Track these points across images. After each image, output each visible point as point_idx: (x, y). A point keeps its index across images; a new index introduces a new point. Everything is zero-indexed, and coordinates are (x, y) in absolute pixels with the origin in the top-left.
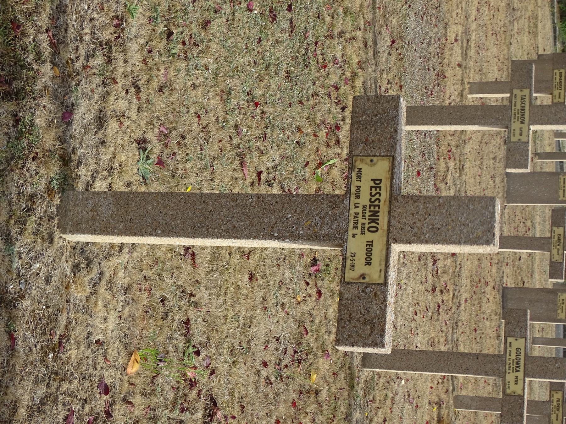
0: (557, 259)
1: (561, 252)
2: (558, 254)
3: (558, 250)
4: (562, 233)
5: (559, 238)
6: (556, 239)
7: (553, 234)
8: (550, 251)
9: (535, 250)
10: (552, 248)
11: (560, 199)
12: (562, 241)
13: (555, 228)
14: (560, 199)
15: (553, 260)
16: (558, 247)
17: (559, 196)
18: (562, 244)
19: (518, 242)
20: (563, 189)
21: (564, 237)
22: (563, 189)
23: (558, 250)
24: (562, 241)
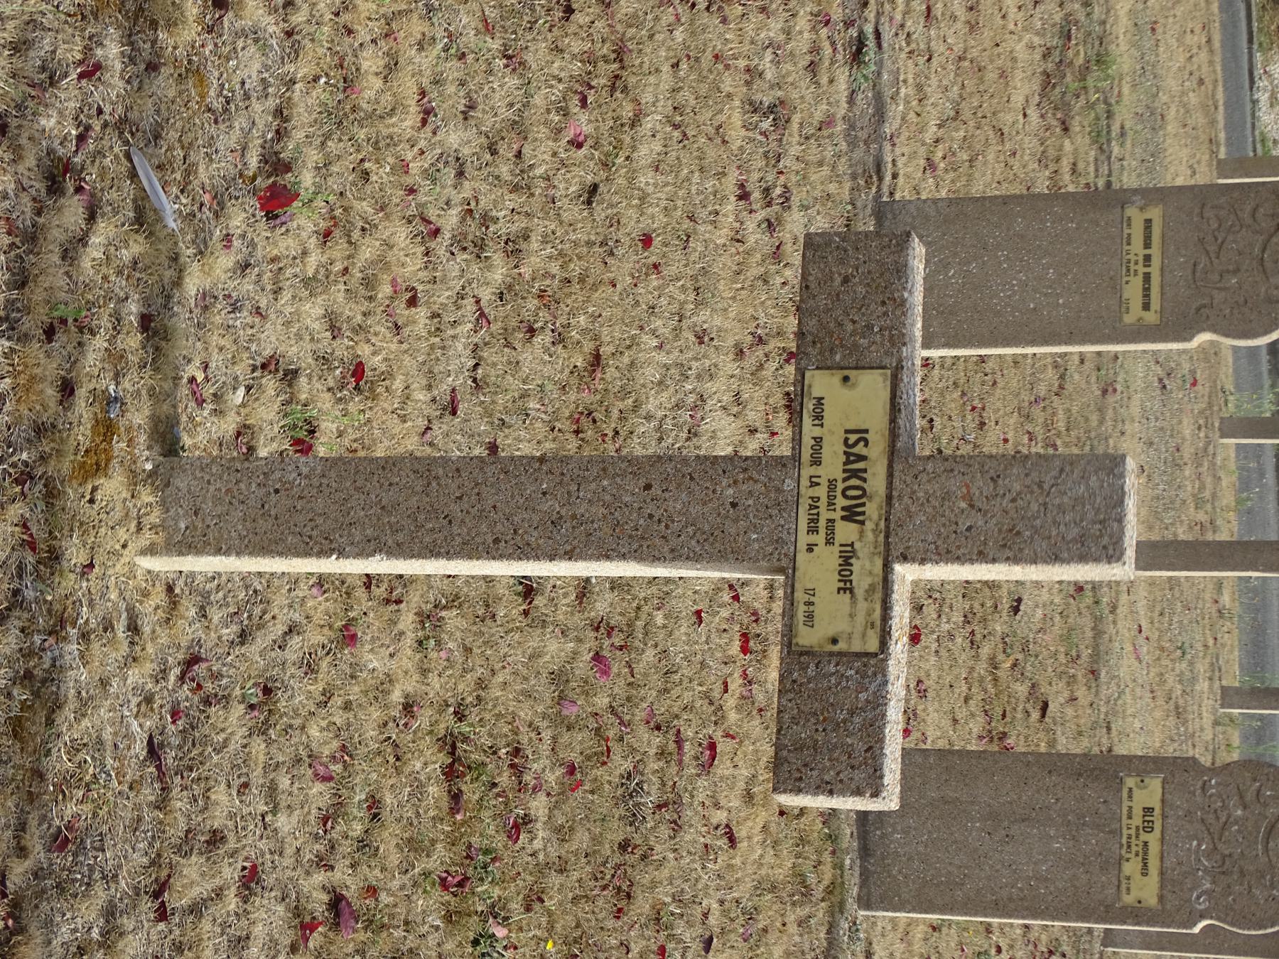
0: (840, 625)
1: (865, 569)
2: (846, 587)
3: (847, 558)
4: (877, 423)
5: (851, 458)
6: (832, 466)
7: (809, 430)
8: (789, 569)
9: (675, 556)
10: (804, 539)
11: (1128, 319)
12: (876, 481)
13: (822, 383)
14: (1128, 319)
15: (807, 637)
16: (846, 532)
17: (1123, 305)
18: (872, 509)
19: (548, 505)
20: (1142, 270)
21: (892, 452)
22: (1142, 270)
23: (847, 558)
24: (876, 481)
